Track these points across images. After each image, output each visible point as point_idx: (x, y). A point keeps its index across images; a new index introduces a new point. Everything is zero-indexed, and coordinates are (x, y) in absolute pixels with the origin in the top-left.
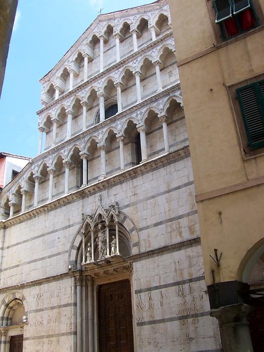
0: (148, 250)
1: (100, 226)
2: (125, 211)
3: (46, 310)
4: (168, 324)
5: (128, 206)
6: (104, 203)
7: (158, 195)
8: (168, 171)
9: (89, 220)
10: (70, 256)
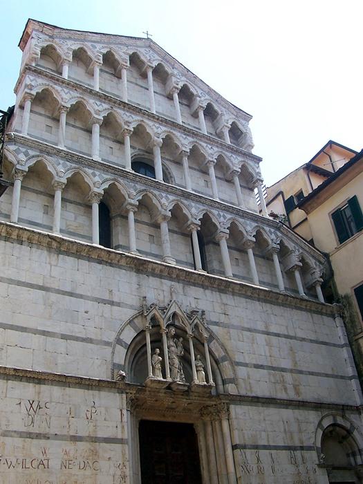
7: (258, 331)
8: (265, 309)
9: (158, 314)
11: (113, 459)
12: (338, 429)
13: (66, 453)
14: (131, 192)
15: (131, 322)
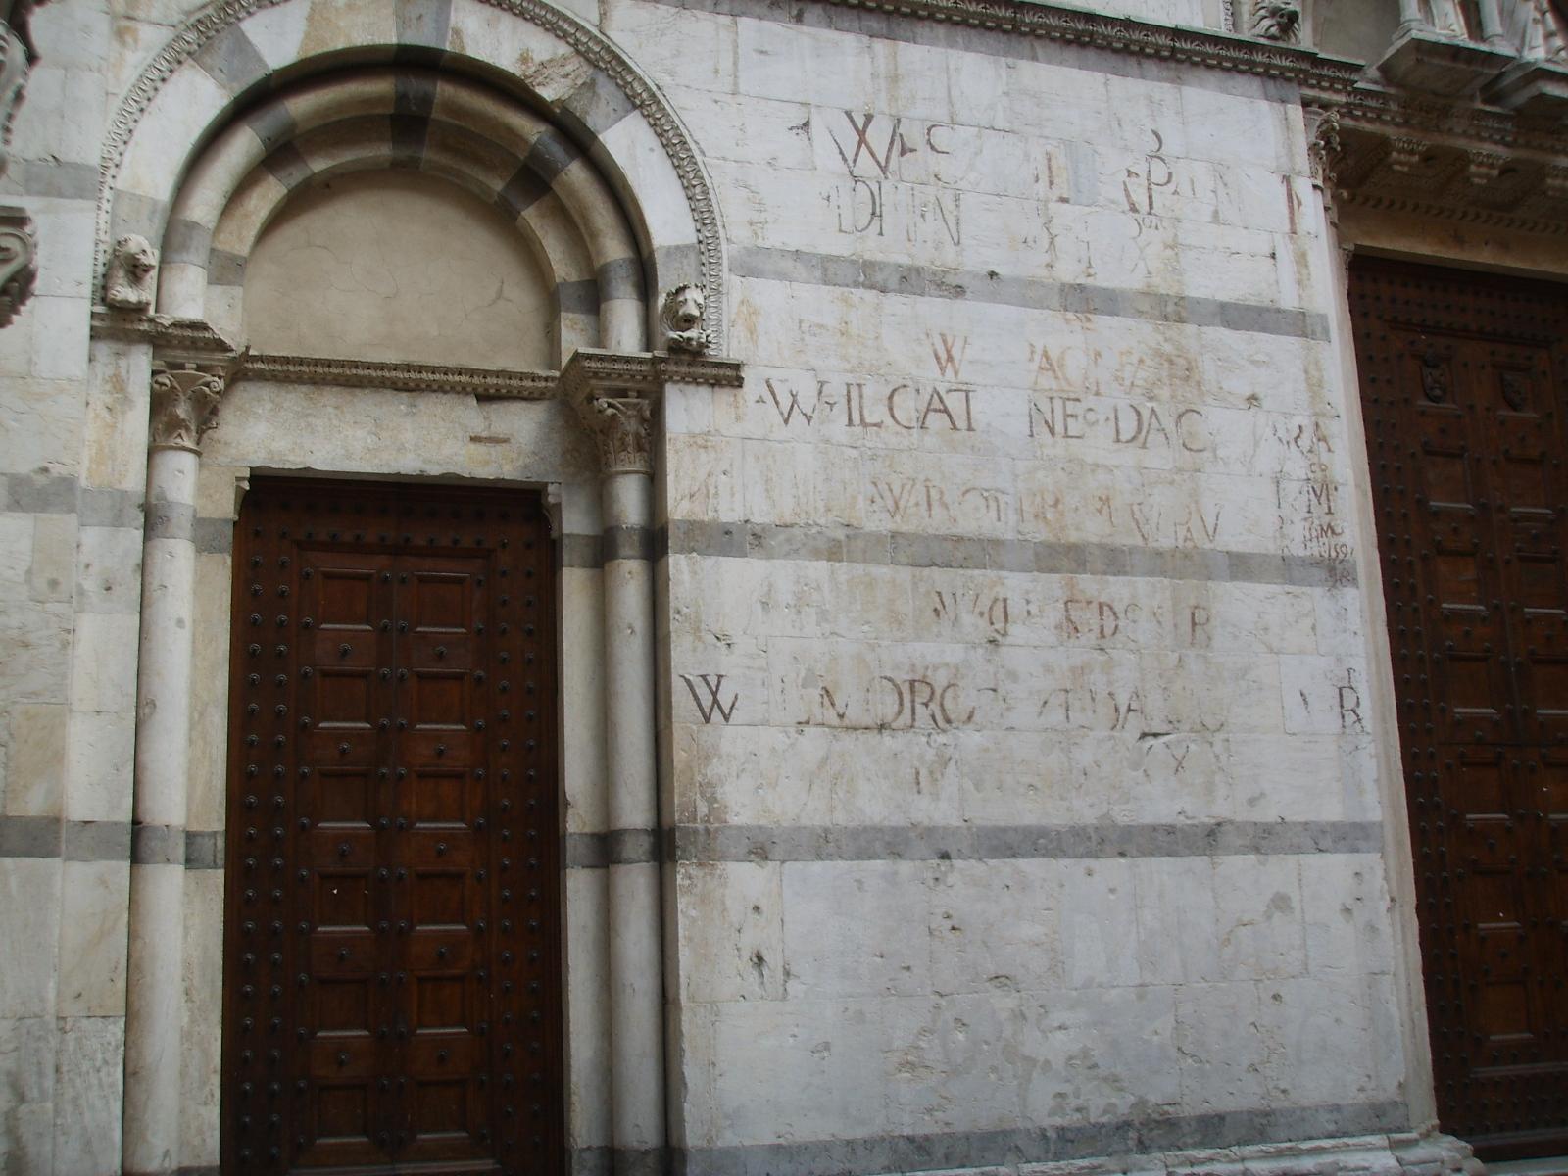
3: (993, 298)
11: (1266, 404)
13: (1049, 365)
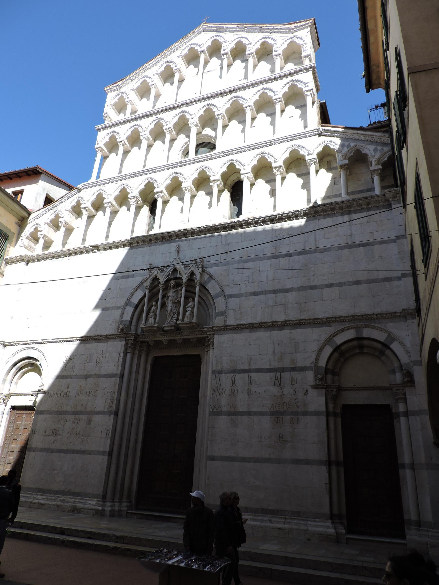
0: (238, 322)
1: (172, 283)
2: (211, 270)
4: (255, 419)
5: (216, 265)
6: (181, 256)
10: (123, 314)
12: (365, 342)
14: (162, 182)
15: (141, 285)
